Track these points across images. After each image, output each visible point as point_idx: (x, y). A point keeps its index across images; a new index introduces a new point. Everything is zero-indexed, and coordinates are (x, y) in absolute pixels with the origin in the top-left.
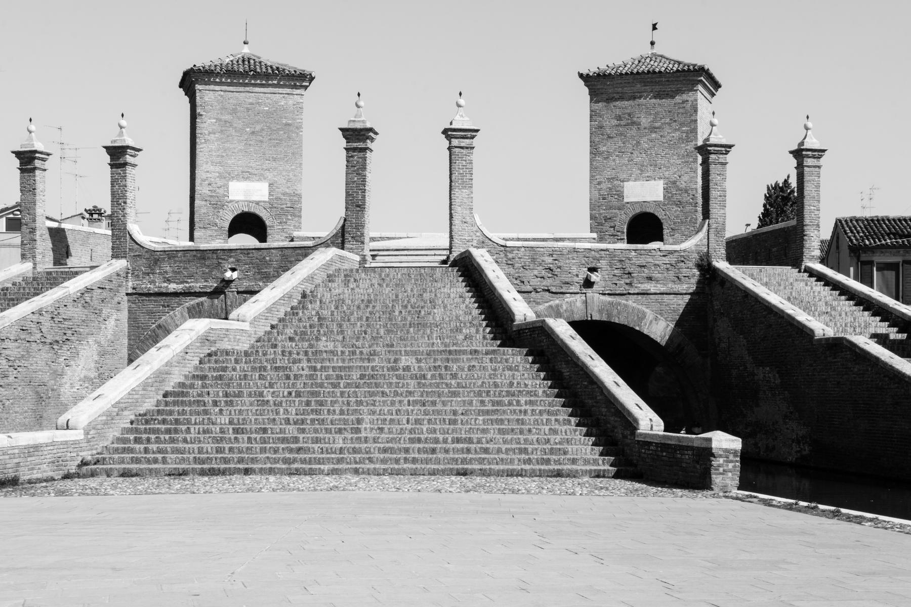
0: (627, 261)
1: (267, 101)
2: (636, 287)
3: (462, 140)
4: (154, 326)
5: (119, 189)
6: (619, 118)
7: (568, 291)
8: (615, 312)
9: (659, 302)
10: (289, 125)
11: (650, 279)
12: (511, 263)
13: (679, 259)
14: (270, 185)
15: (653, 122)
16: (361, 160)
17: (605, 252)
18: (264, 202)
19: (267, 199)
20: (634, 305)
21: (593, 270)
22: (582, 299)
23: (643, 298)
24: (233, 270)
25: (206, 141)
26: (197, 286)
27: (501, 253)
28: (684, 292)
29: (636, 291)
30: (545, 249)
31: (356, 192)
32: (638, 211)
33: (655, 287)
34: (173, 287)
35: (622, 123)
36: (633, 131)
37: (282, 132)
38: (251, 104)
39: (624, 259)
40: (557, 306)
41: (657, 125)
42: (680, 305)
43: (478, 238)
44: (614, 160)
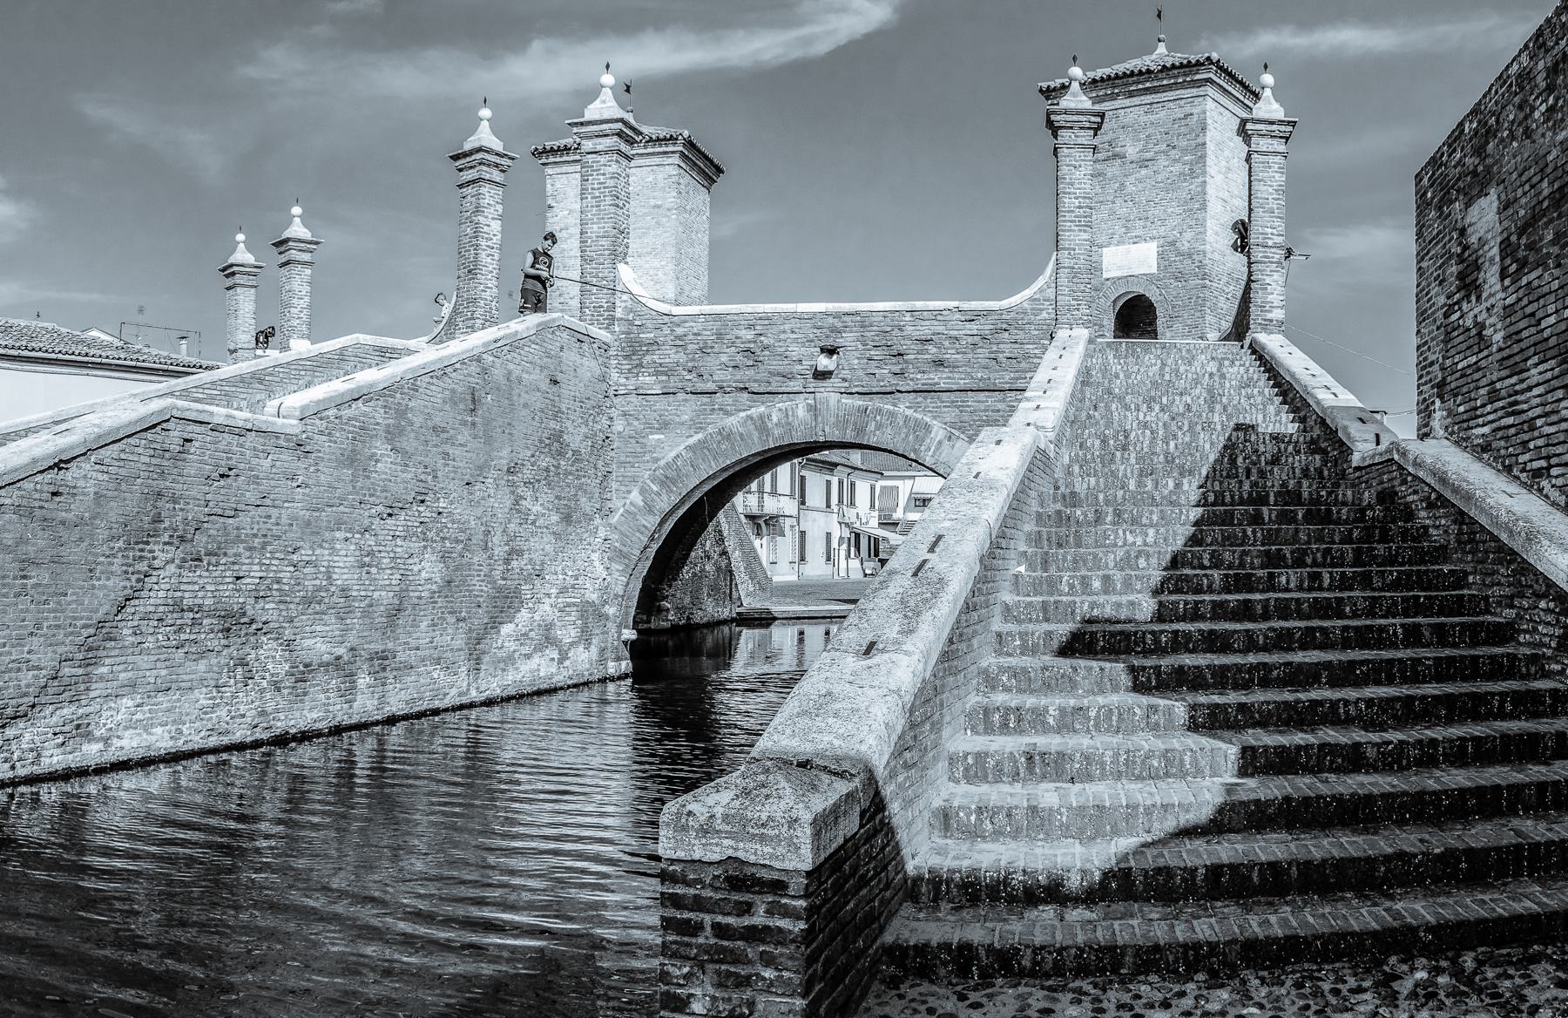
0: (896, 332)
2: (912, 380)
7: (781, 390)
8: (872, 427)
9: (958, 407)
11: (939, 363)
12: (681, 343)
13: (999, 326)
17: (853, 318)
20: (909, 412)
21: (831, 351)
22: (808, 404)
23: (925, 398)
27: (665, 328)
28: (1007, 386)
29: (911, 386)
30: (741, 317)
33: (949, 378)
39: (889, 329)
40: (761, 417)
42: (998, 411)
43: (623, 305)
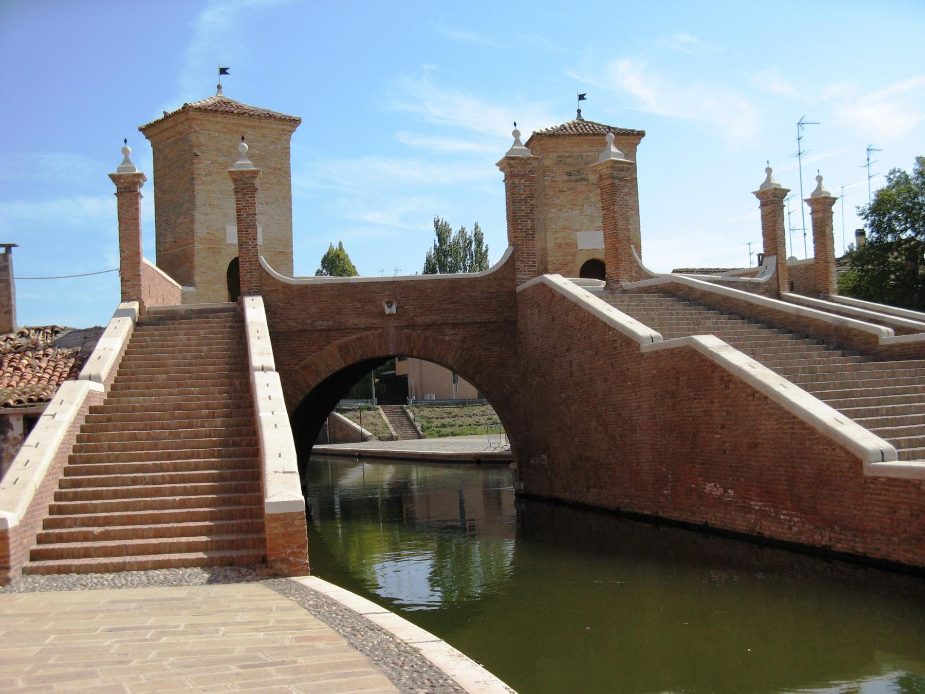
1: (258, 144)
3: (619, 173)
4: (297, 367)
5: (249, 218)
6: (569, 174)
10: (279, 169)
16: (528, 189)
24: (390, 304)
25: (203, 183)
26: (352, 321)
31: (525, 221)
32: (591, 257)
34: (319, 324)
36: (581, 187)
37: (273, 176)
43: (635, 269)
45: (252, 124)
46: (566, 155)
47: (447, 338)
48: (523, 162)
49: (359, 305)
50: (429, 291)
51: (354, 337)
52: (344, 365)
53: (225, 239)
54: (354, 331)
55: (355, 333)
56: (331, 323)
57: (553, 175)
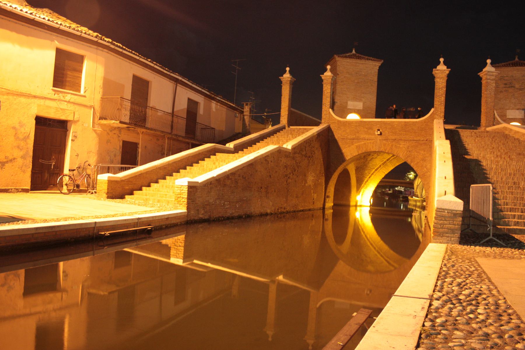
10: (372, 80)
14: (364, 104)
15: (520, 86)
18: (361, 110)
19: (362, 109)
34: (349, 137)
35: (507, 86)
36: (511, 90)
38: (357, 71)
41: (522, 88)
44: (503, 101)
45: (362, 62)
46: (505, 75)
47: (401, 146)
48: (442, 71)
49: (366, 130)
50: (396, 126)
51: (363, 143)
52: (357, 154)
53: (347, 106)
54: (363, 140)
55: (363, 141)
56: (354, 136)
57: (498, 84)
